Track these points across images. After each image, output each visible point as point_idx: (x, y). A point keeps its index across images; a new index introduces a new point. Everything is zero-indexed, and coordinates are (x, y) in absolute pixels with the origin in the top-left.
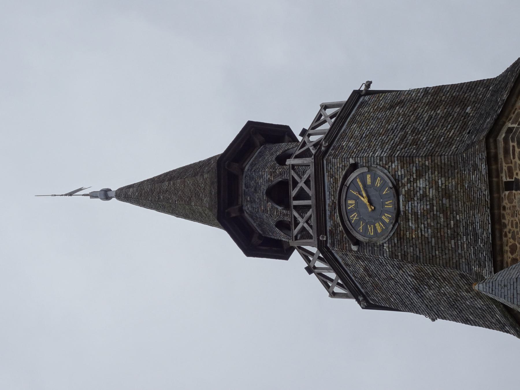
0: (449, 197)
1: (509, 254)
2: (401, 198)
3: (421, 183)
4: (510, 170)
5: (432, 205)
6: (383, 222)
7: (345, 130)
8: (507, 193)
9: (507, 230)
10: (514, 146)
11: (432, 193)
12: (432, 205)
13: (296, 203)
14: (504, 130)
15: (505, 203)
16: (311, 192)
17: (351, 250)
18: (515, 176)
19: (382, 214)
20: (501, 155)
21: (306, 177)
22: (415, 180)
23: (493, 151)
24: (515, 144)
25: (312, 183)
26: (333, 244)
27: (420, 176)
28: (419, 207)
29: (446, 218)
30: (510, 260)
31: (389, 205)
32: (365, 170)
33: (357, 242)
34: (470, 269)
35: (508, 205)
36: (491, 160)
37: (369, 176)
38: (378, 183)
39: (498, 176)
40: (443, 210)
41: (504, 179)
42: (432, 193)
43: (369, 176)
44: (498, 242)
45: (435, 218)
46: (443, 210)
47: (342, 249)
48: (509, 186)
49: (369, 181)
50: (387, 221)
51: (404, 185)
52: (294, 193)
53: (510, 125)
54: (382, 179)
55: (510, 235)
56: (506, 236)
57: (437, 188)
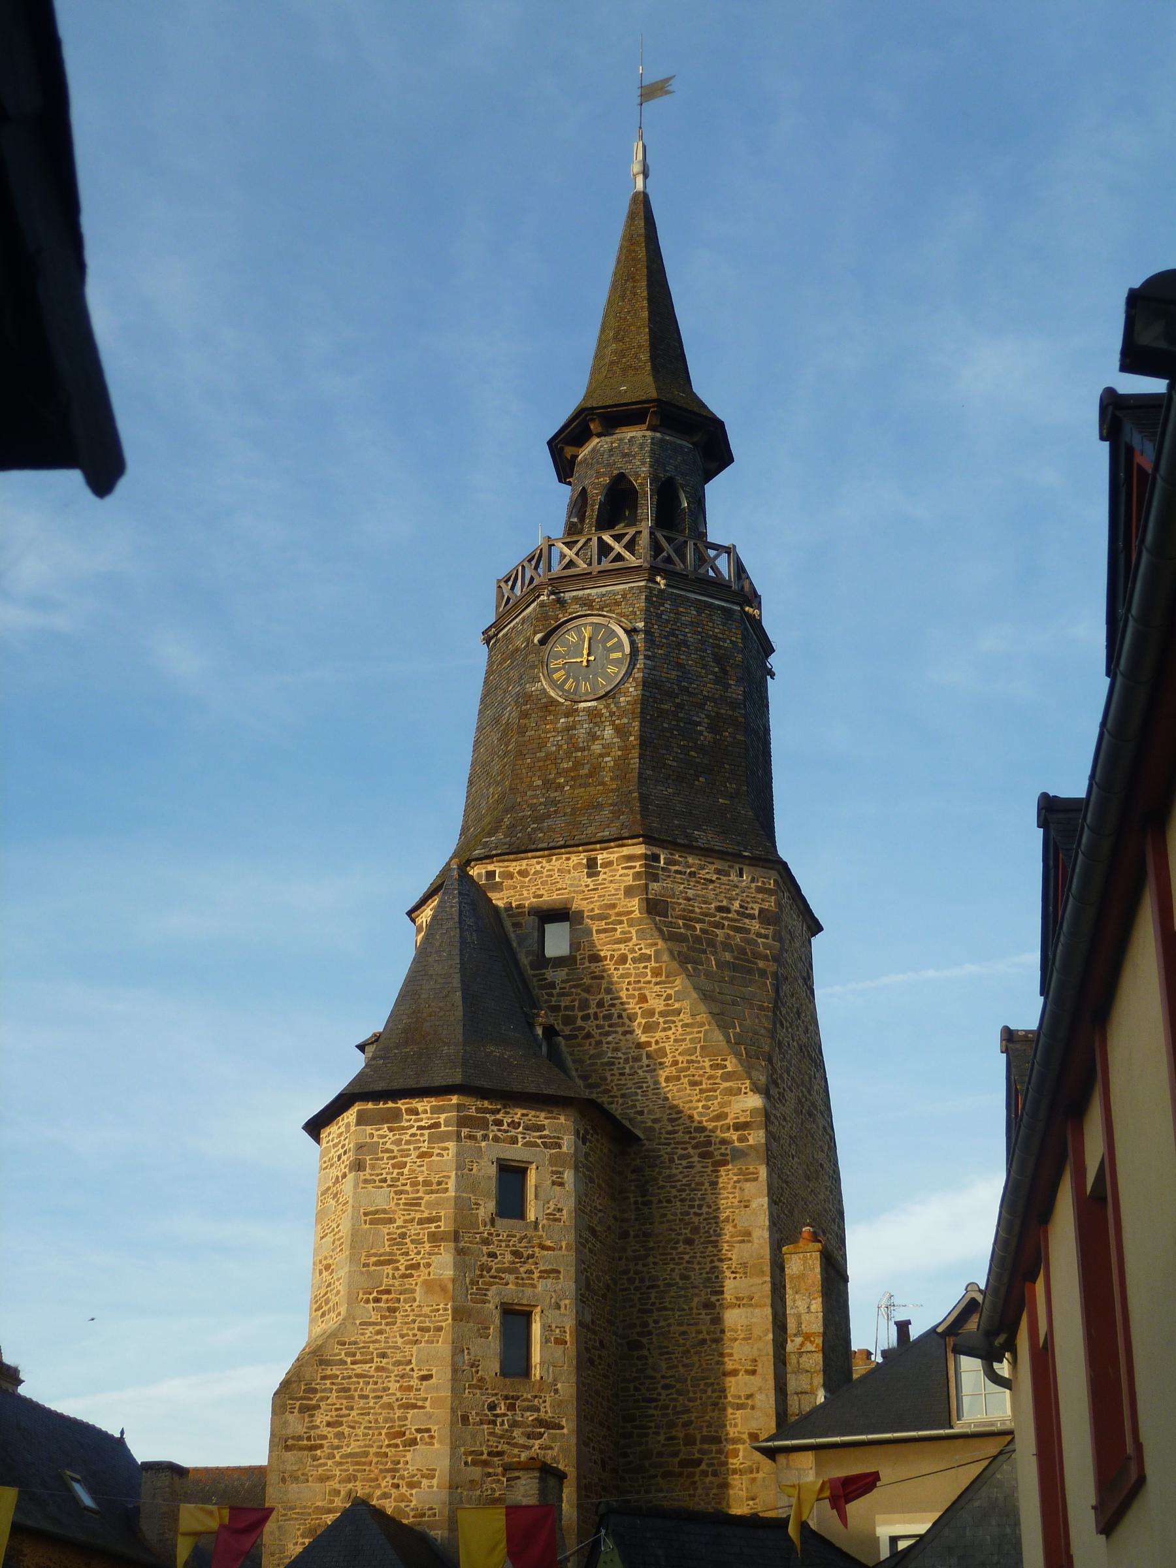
0: (590, 775)
1: (518, 869)
2: (594, 703)
3: (609, 732)
4: (610, 863)
5: (583, 750)
6: (566, 681)
7: (688, 598)
8: (585, 861)
9: (544, 863)
10: (635, 867)
11: (597, 748)
12: (583, 750)
13: (595, 539)
14: (656, 850)
15: (574, 859)
16: (606, 564)
17: (535, 634)
18: (604, 870)
19: (576, 679)
20: (626, 851)
21: (626, 555)
22: (613, 723)
23: (630, 841)
24: (637, 869)
25: (618, 565)
26: (542, 605)
27: (620, 731)
28: (581, 732)
29: (567, 771)
30: (511, 869)
31: (585, 687)
32: (627, 650)
33: (543, 642)
34: (507, 811)
35: (571, 863)
36: (618, 840)
37: (619, 655)
38: (611, 669)
39: (602, 849)
40: (578, 764)
41: (599, 857)
42: (597, 748)
43: (619, 655)
44: (530, 854)
45: (568, 755)
46: (578, 764)
47: (537, 619)
48: (591, 864)
49: (614, 656)
50: (566, 687)
51: (607, 707)
52: (607, 538)
53: (662, 857)
54: (617, 674)
55: (538, 867)
56: (538, 863)
57: (602, 756)
